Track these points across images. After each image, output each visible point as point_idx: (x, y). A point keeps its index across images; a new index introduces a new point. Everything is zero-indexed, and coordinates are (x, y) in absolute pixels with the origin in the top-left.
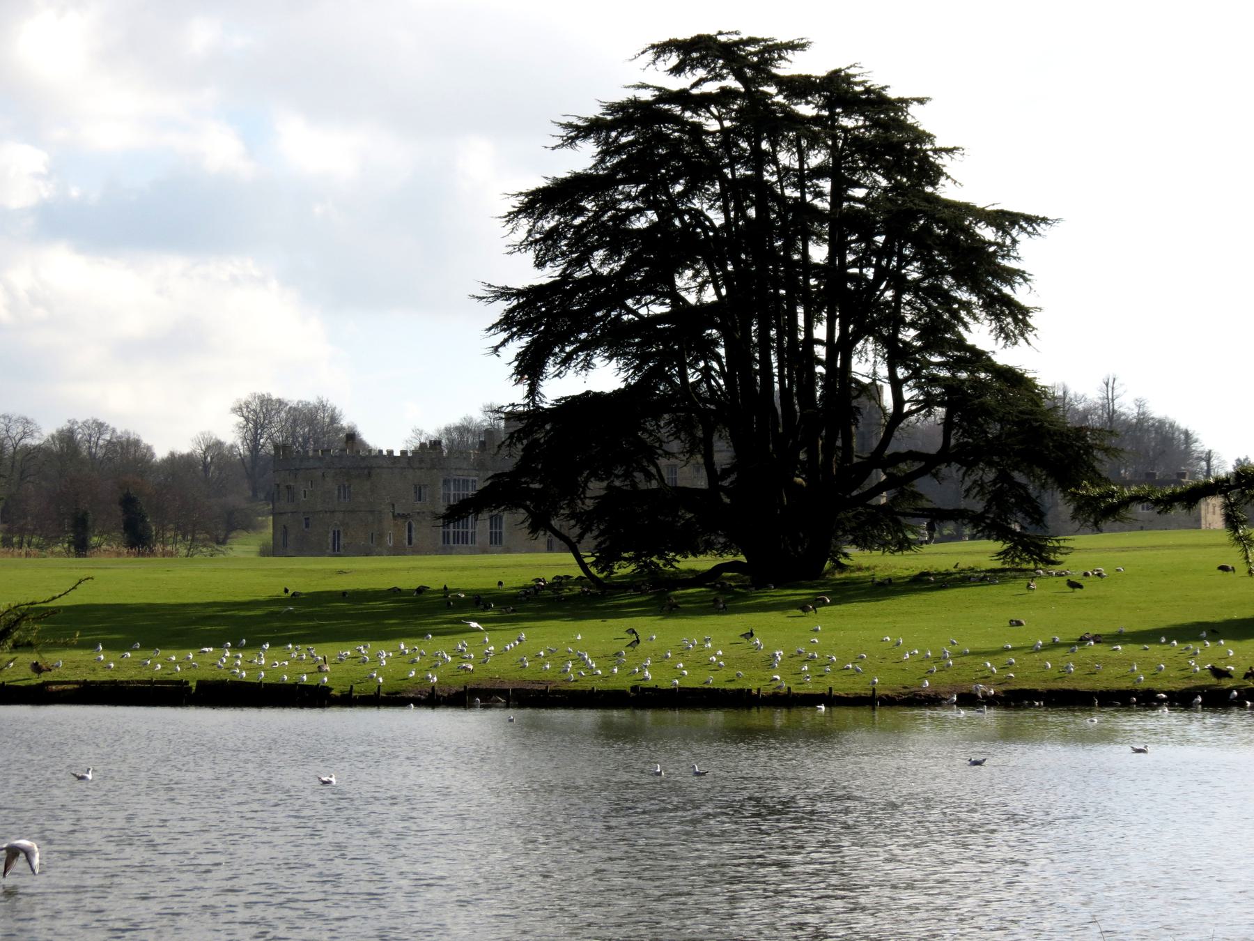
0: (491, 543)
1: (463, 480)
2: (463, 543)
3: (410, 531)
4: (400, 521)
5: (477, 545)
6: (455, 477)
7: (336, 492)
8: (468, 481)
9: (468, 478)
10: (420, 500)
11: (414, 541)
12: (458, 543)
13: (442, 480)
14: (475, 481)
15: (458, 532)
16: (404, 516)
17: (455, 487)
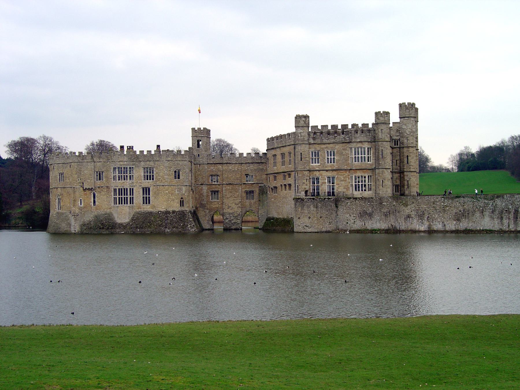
0: (144, 203)
1: (124, 168)
2: (125, 204)
3: (94, 197)
4: (88, 192)
5: (134, 204)
6: (120, 166)
7: (59, 177)
8: (127, 168)
9: (126, 166)
10: (100, 180)
11: (96, 203)
12: (122, 204)
13: (112, 168)
14: (133, 168)
15: (122, 198)
16: (90, 189)
17: (119, 171)
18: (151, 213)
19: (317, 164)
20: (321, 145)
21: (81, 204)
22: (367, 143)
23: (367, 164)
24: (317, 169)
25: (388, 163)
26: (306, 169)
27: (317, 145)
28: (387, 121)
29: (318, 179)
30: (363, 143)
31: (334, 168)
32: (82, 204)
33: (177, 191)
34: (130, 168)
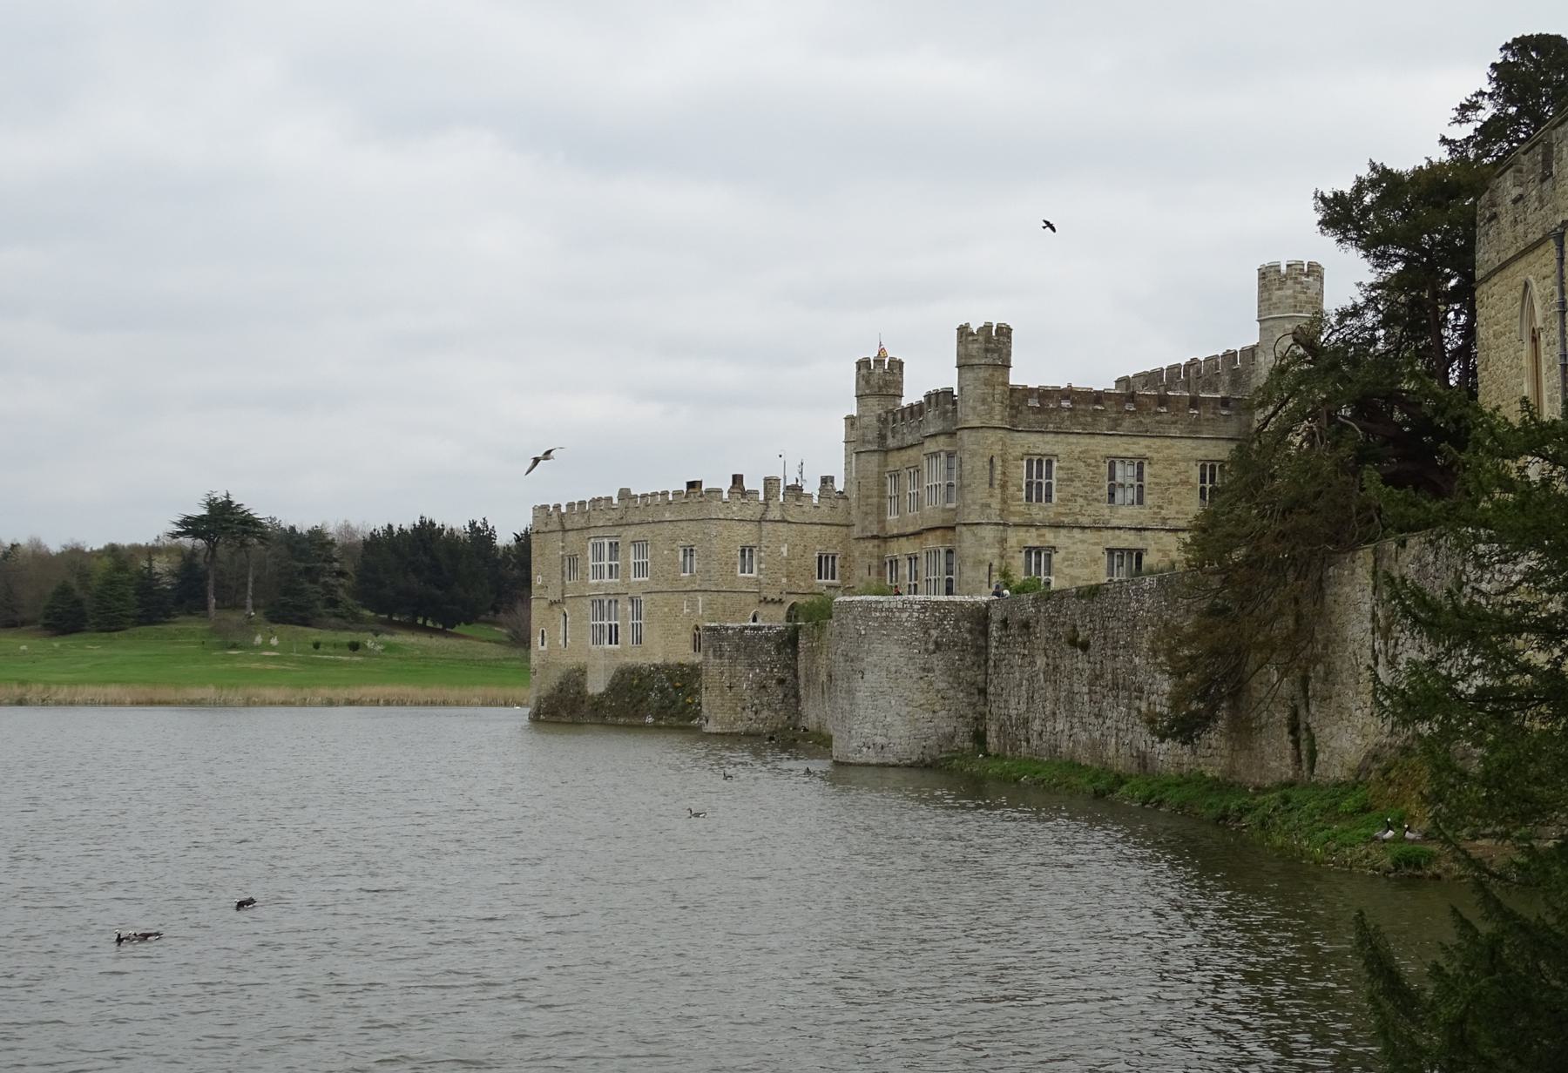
11: (568, 640)
14: (617, 543)
18: (635, 671)
19: (896, 517)
20: (903, 452)
21: (543, 644)
22: (942, 439)
23: (944, 510)
24: (895, 532)
25: (974, 503)
26: (869, 534)
27: (895, 453)
28: (973, 357)
29: (896, 561)
30: (938, 438)
31: (918, 528)
32: (546, 643)
33: (688, 607)
34: (611, 544)
